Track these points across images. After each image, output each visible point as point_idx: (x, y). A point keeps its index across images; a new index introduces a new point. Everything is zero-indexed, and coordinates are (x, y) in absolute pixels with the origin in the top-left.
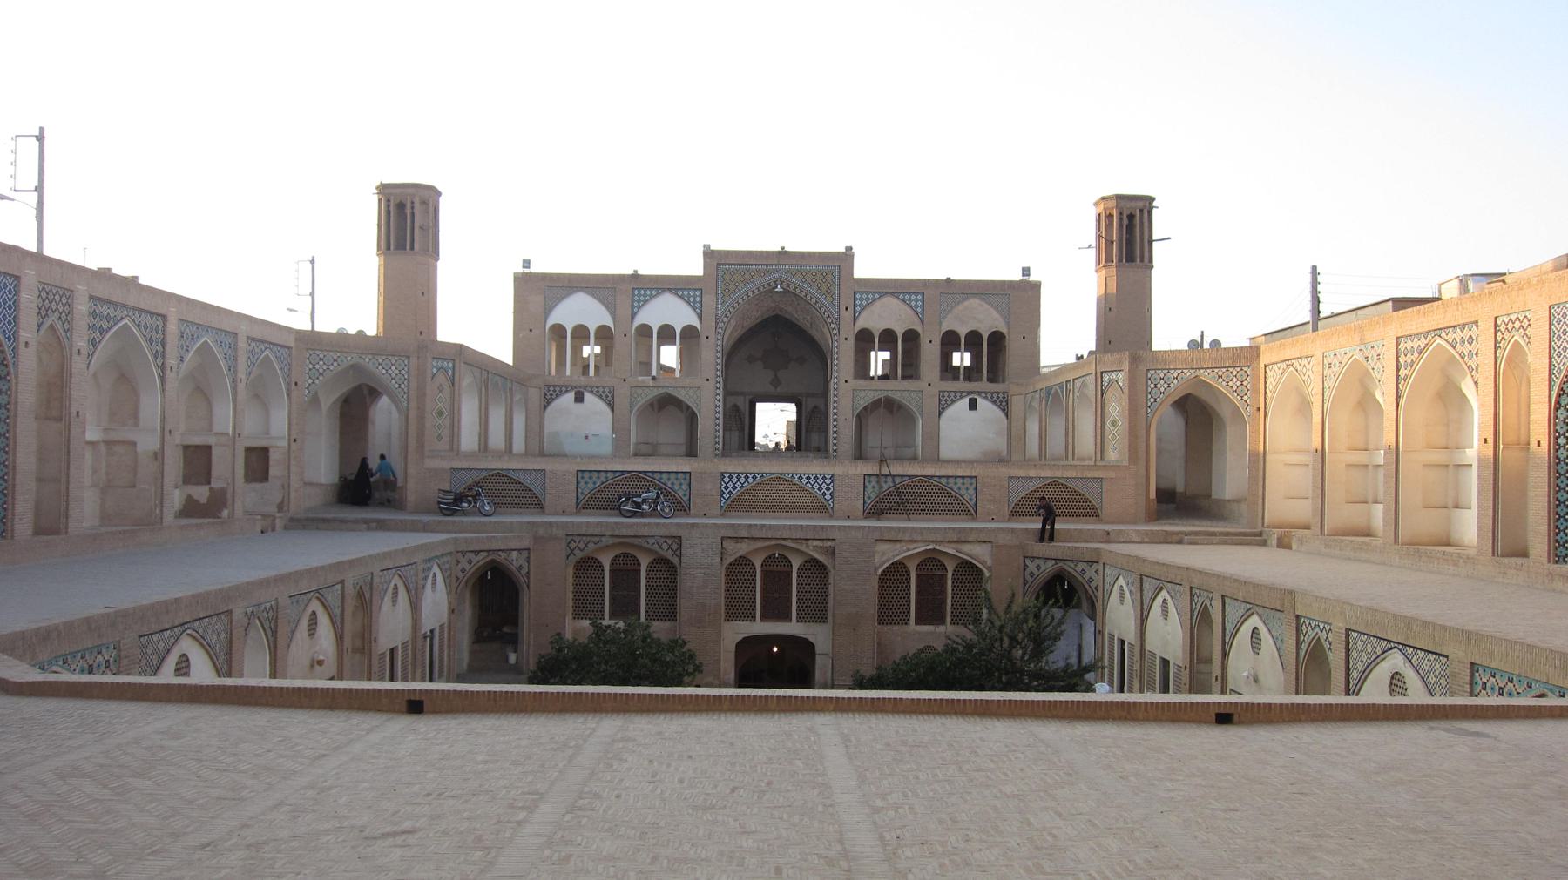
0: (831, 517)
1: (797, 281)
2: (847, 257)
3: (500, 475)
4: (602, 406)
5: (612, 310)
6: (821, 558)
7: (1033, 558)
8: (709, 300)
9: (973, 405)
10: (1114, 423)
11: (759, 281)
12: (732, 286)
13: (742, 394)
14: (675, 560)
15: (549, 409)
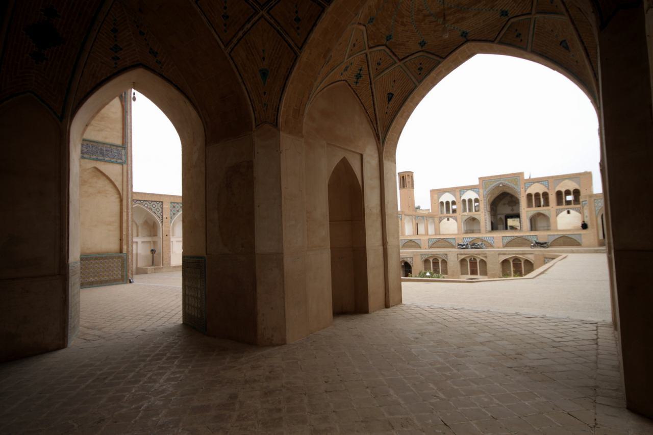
0: (494, 248)
1: (506, 182)
2: (522, 174)
3: (411, 241)
4: (455, 221)
5: (455, 196)
6: (484, 259)
7: (547, 258)
8: (481, 191)
9: (569, 212)
10: (587, 217)
11: (495, 184)
12: (487, 186)
13: (503, 214)
14: (446, 260)
15: (442, 222)
